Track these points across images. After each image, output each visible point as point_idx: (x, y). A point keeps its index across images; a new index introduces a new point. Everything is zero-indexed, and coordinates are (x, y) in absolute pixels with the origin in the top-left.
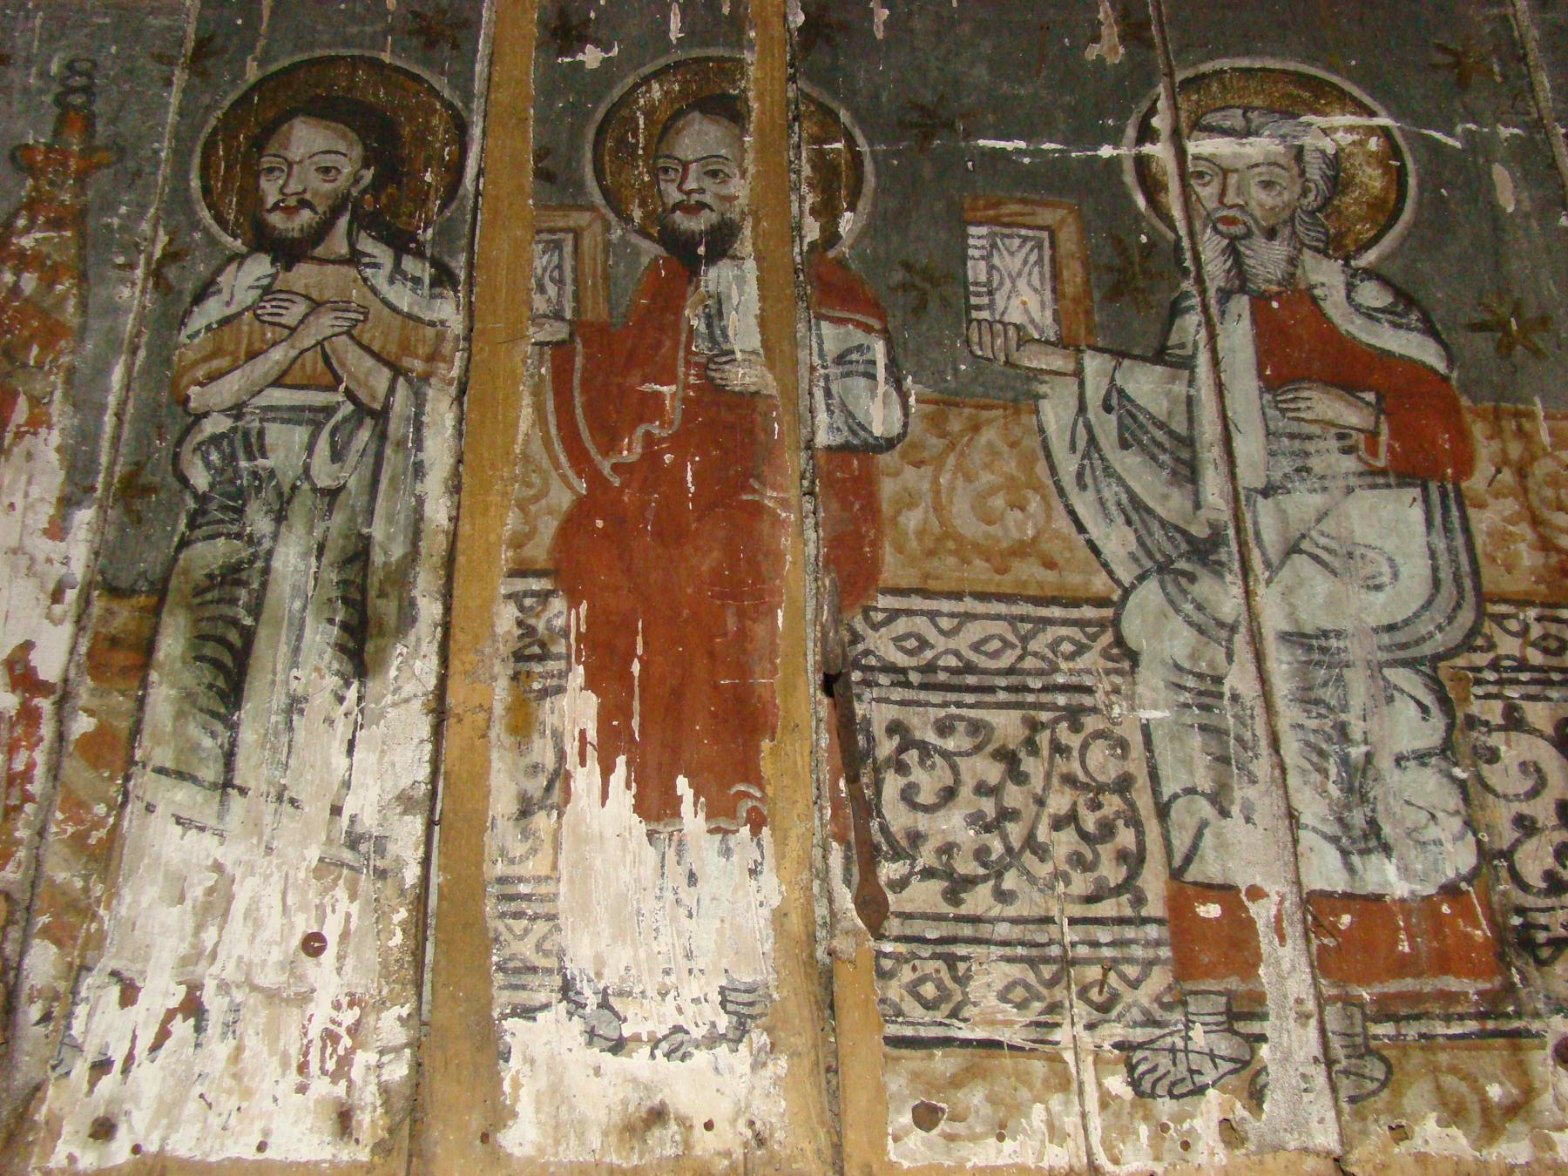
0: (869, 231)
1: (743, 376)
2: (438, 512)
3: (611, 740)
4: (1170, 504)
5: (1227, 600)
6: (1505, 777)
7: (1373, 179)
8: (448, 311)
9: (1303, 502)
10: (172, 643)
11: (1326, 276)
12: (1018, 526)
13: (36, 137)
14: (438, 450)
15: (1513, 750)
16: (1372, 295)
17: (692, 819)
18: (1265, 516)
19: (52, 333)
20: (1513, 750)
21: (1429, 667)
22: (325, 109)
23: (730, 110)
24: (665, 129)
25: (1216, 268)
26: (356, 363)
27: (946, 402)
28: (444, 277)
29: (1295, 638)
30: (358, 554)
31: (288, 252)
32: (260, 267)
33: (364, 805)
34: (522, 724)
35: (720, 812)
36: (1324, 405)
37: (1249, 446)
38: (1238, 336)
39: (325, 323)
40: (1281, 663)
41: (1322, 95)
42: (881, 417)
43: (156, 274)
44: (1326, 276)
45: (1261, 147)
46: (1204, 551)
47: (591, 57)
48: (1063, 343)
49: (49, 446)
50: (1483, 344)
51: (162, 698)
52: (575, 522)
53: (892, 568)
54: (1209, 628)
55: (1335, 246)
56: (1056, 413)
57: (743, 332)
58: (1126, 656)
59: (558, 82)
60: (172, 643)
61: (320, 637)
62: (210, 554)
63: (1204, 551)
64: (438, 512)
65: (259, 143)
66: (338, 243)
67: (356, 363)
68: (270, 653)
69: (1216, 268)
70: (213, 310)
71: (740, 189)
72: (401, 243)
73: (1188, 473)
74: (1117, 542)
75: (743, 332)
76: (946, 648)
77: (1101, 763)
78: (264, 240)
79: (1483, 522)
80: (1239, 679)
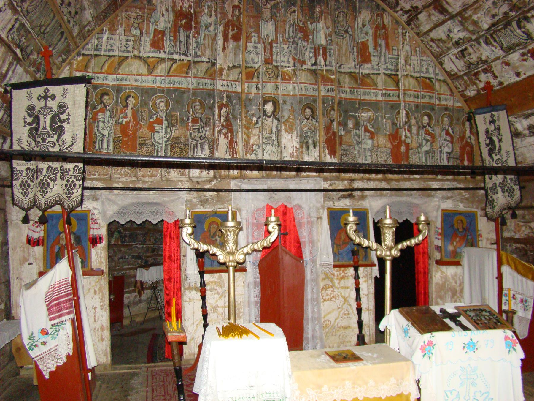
0: (343, 119)
1: (335, 130)
2: (318, 138)
3: (328, 153)
4: (358, 140)
5: (360, 146)
6: (373, 157)
7: (372, 117)
8: (317, 124)
9: (365, 140)
10: (304, 146)
11: (368, 125)
12: (350, 141)
13: (290, 109)
14: (318, 134)
15: (374, 156)
16: (371, 126)
17: (333, 158)
18: (363, 141)
19: (294, 124)
20: (374, 156)
21: (370, 151)
22: (309, 108)
23: (333, 110)
24: (330, 112)
25: (362, 124)
26: (312, 128)
27: (346, 132)
28: (317, 121)
29: (364, 149)
30: (314, 141)
31: (308, 119)
32: (306, 120)
33: (316, 156)
34: (324, 152)
35: (334, 157)
36: (368, 134)
37: (363, 136)
38: (363, 128)
39: (310, 125)
40: (363, 150)
41: (369, 111)
42: (343, 134)
43: (299, 120)
44: (368, 125)
45: (366, 115)
46: (360, 143)
47: (325, 105)
48: (353, 129)
49: (295, 132)
50: (376, 130)
51: (304, 149)
52: (326, 139)
53: (343, 143)
54: (360, 148)
55: (369, 122)
56: (352, 133)
57: (335, 127)
58: (355, 149)
59: (324, 107)
60: (304, 146)
61: (312, 146)
62: (306, 141)
63: (360, 143)
64: (318, 138)
65: (305, 110)
66: (310, 119)
67: (312, 128)
68: (310, 147)
69: (362, 124)
70: (303, 123)
71: (335, 116)
72: (314, 119)
73: (359, 138)
74: (355, 142)
75: (335, 127)
76: (346, 148)
77: (353, 155)
78: (306, 118)
79: (375, 142)
80: (361, 151)
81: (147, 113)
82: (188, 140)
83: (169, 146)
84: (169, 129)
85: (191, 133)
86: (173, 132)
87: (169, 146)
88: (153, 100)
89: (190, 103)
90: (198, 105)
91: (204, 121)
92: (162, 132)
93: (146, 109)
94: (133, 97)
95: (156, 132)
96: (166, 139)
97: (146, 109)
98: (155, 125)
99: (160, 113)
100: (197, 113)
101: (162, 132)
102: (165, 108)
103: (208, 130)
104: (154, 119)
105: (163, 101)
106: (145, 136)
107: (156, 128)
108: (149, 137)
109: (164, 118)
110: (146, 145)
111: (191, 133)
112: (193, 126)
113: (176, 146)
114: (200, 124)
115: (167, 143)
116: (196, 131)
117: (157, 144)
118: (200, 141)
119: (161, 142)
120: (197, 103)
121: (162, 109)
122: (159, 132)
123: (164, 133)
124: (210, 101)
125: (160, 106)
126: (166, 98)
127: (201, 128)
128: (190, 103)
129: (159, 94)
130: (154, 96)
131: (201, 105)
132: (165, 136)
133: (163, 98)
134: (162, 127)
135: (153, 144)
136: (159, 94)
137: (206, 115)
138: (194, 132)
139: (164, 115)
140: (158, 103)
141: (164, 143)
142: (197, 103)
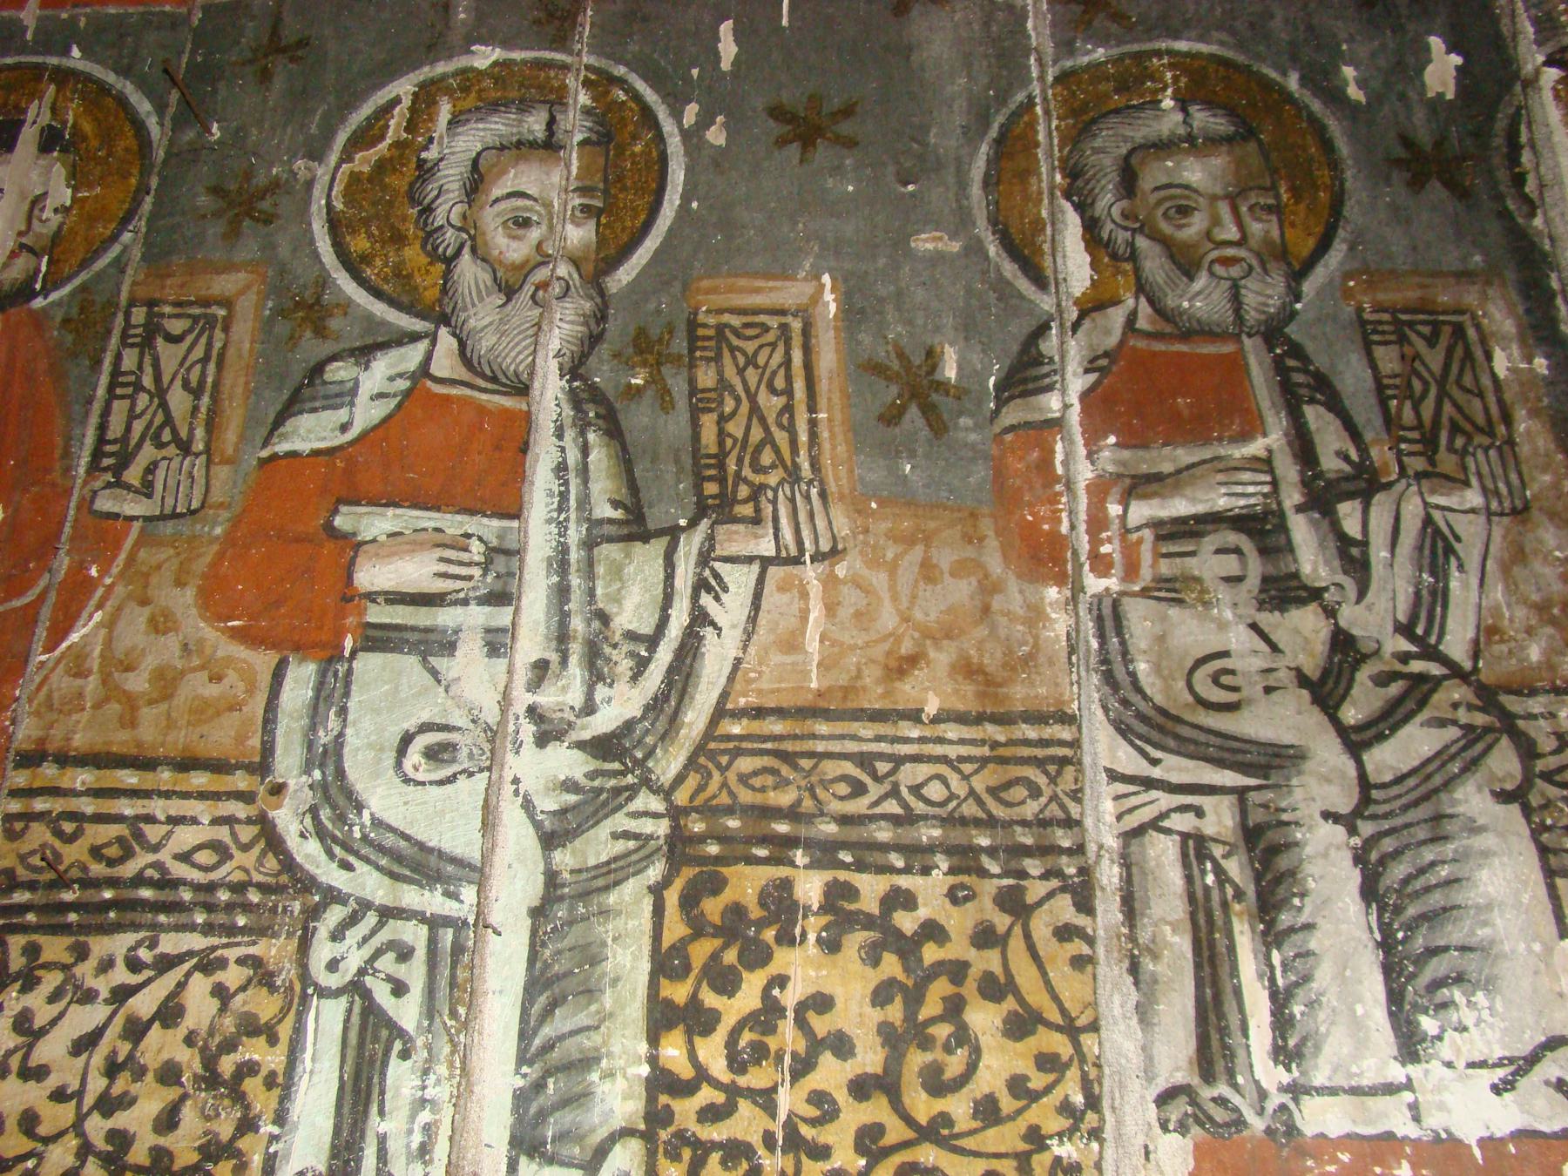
81: (244, 330)
82: (1066, 760)
83: (632, 897)
84: (645, 561)
85: (1110, 618)
86: (730, 611)
87: (632, 897)
88: (365, 137)
89: (1047, 132)
90: (1191, 143)
91: (1353, 377)
92: (497, 643)
93: (224, 284)
94: (50, 141)
95: (380, 639)
96: (565, 761)
97: (224, 284)
98: (375, 524)
99: (482, 315)
100: (1185, 262)
101: (497, 643)
102: (578, 235)
103: (1470, 531)
104: (366, 414)
105: (550, 145)
106: (148, 732)
107: (372, 576)
108: (219, 738)
109: (550, 391)
110: (97, 918)
111: (1110, 618)
112: (1139, 485)
113: (780, 903)
114: (1273, 439)
115: (599, 845)
116: (1208, 563)
117: (369, 883)
118: (1328, 753)
119: (461, 839)
120: (1168, 118)
121: (515, 250)
122: (441, 644)
123: (531, 645)
124: (1412, 63)
125: (491, 220)
126: (600, 83)
127: (1321, 500)
128: (1047, 132)
129: (485, 57)
130: (404, 88)
131: (1245, 132)
132: (565, 692)
133: (556, 100)
134: (505, 554)
135: (297, 879)
136: (485, 57)
137: (1372, 275)
138: (1171, 591)
139: (562, 331)
140: (452, 177)
141: (517, 834)
142: (1168, 118)
